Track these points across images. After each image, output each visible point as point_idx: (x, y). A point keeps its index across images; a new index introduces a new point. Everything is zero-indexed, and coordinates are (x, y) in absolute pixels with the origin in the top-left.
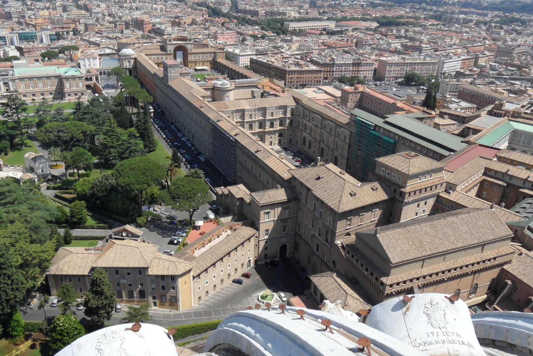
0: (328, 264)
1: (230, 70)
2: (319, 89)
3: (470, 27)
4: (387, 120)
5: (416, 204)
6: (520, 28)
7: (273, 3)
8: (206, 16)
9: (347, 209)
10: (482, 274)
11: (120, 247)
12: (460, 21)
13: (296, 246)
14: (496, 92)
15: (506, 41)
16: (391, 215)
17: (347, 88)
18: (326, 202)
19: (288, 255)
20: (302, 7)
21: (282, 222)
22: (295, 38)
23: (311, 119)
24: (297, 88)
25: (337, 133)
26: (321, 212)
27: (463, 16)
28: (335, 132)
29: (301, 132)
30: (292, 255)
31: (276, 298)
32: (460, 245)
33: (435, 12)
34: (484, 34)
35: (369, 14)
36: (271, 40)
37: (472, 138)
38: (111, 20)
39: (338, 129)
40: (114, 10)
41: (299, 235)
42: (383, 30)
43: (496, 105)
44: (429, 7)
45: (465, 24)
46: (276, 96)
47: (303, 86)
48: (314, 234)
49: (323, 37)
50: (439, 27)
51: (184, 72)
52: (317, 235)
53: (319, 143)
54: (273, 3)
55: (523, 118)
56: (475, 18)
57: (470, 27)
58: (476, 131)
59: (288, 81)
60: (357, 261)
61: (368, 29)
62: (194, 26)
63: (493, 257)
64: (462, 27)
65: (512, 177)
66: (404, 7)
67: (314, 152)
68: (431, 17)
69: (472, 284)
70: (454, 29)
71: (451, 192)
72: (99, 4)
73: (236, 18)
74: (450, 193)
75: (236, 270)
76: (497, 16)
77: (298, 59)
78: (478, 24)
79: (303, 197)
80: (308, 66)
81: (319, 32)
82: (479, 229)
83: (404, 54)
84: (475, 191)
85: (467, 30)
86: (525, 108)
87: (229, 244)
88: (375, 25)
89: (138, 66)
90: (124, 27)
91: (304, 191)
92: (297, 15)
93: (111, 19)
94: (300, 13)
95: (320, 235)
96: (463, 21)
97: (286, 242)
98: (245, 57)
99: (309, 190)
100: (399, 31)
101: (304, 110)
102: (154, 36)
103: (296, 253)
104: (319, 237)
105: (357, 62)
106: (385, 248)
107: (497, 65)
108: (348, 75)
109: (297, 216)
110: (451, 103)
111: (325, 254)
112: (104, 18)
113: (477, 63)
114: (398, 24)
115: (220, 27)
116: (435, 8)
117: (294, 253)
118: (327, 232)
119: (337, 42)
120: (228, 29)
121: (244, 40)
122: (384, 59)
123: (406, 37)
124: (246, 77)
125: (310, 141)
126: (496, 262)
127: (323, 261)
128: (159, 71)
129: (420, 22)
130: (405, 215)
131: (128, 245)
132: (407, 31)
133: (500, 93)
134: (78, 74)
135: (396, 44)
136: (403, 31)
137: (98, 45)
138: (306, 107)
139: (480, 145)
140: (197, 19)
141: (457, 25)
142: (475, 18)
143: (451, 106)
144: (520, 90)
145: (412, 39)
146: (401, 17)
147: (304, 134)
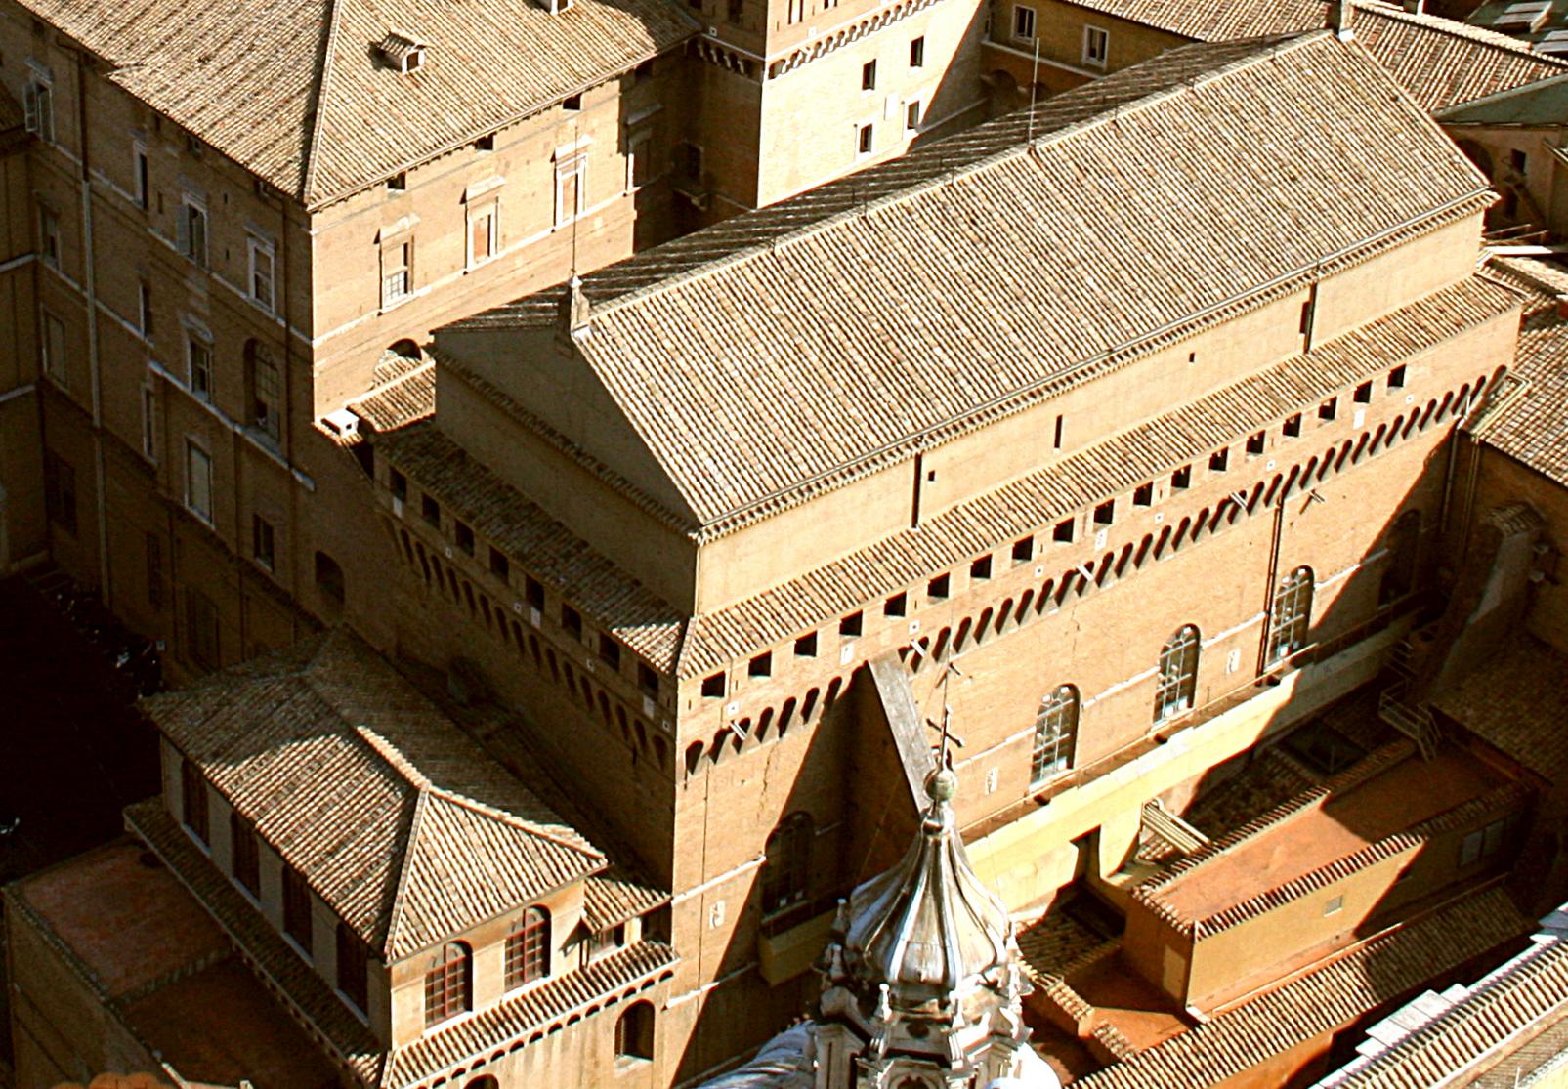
10: (1330, 485)
26: (194, 213)
52: (185, 388)
69: (1272, 575)
79: (61, 125)
91: (56, 78)
95: (201, 380)
99: (90, 64)
104: (201, 399)
109: (35, 267)
118: (250, 351)
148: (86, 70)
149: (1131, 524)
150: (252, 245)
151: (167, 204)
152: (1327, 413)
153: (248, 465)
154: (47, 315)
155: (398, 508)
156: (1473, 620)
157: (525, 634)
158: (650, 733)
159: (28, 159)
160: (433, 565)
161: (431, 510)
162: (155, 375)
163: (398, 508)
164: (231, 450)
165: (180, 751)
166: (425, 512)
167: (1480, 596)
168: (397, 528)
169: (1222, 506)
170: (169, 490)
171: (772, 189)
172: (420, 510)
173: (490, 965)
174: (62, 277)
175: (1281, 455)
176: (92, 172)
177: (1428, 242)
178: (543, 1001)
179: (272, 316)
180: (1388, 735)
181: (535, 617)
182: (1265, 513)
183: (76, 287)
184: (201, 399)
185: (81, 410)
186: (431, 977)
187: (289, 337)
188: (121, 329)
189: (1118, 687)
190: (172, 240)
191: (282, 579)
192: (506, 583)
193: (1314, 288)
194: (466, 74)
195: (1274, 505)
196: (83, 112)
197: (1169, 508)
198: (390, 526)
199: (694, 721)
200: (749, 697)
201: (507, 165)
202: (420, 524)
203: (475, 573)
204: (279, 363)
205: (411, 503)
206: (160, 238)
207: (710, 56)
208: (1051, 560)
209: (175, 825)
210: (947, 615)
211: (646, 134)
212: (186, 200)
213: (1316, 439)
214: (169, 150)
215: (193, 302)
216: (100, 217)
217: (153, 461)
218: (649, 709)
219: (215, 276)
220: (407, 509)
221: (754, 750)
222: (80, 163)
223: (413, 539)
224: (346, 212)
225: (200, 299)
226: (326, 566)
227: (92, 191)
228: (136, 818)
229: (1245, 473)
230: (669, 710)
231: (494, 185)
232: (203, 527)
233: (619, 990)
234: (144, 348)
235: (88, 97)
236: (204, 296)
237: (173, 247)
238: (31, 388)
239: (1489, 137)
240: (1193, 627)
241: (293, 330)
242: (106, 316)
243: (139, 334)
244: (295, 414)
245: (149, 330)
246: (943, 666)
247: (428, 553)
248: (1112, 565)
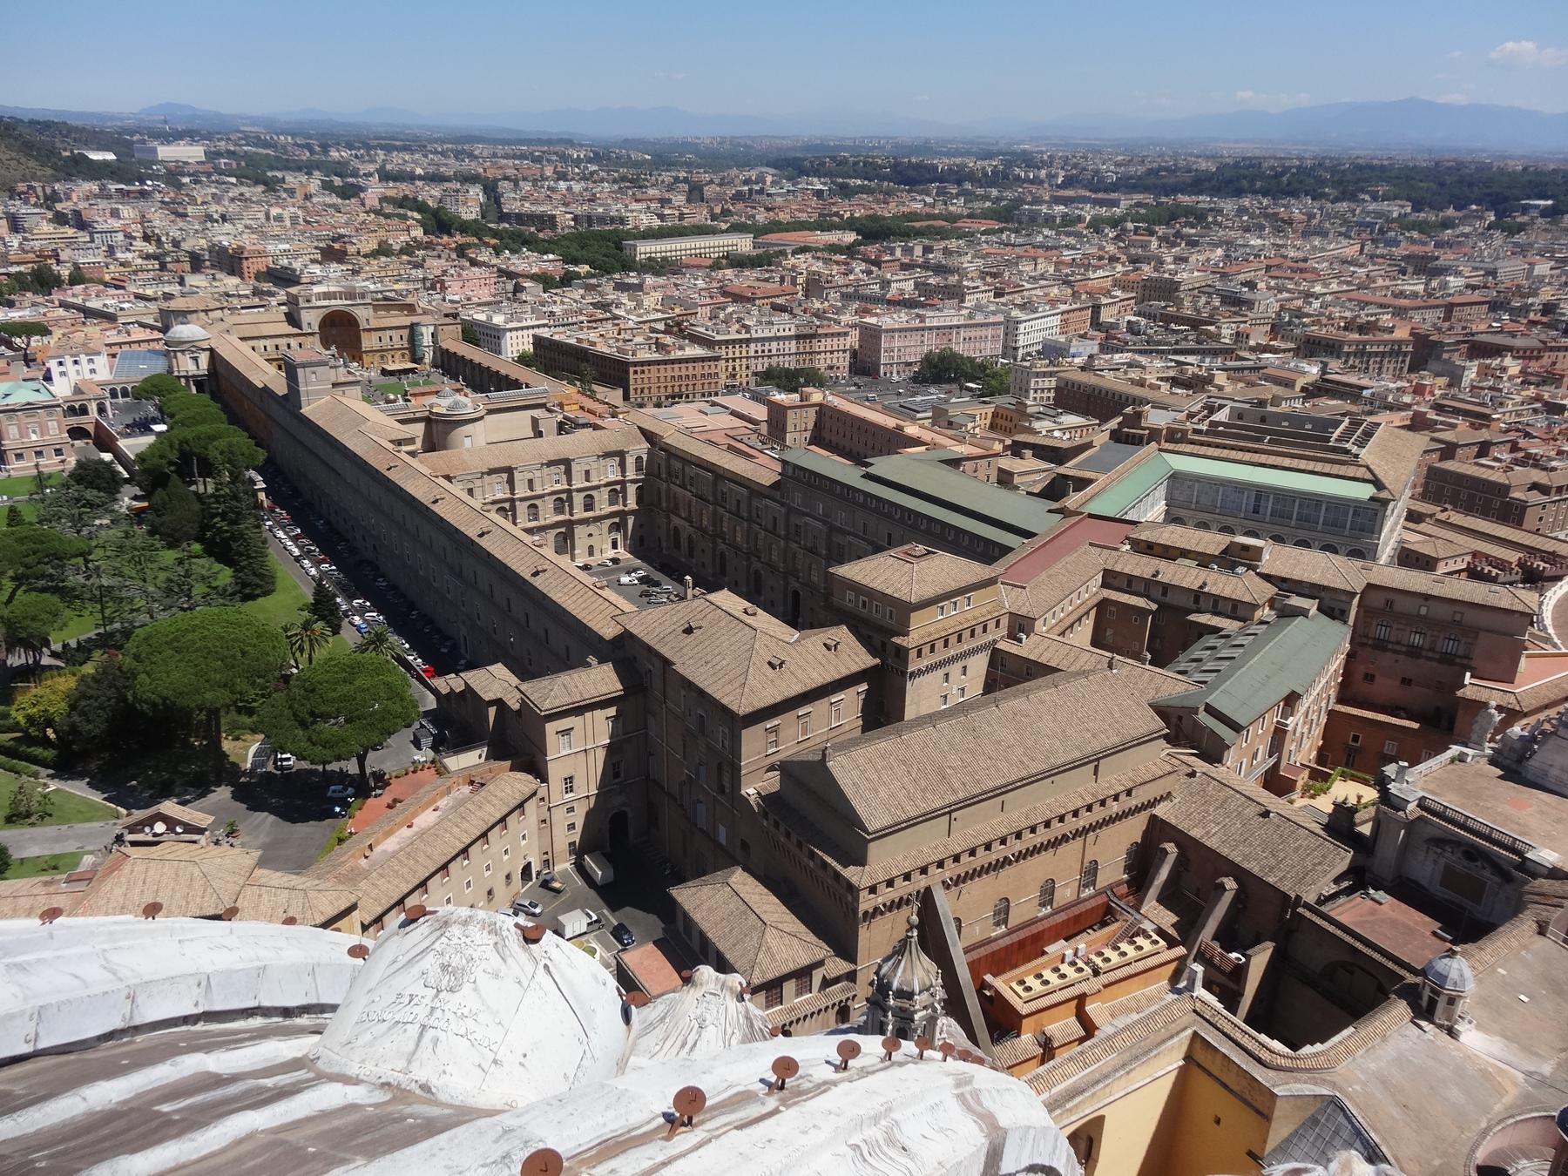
1: (485, 374)
2: (714, 404)
3: (1078, 235)
4: (870, 470)
5: (940, 673)
6: (1193, 231)
7: (594, 195)
8: (418, 233)
10: (1104, 832)
11: (140, 867)
12: (1054, 221)
14: (1143, 386)
15: (1162, 263)
17: (780, 397)
18: (709, 691)
20: (669, 201)
22: (650, 280)
23: (687, 480)
24: (658, 405)
25: (754, 512)
27: (1062, 207)
28: (750, 512)
29: (668, 517)
31: (601, 956)
32: (1035, 767)
33: (999, 199)
34: (1111, 249)
35: (836, 214)
36: (590, 288)
37: (1073, 500)
38: (151, 251)
39: (755, 503)
40: (159, 220)
42: (872, 250)
43: (1125, 415)
44: (980, 191)
45: (1066, 226)
46: (596, 427)
47: (675, 398)
49: (720, 274)
50: (1004, 236)
51: (343, 379)
53: (714, 542)
54: (594, 195)
55: (1193, 442)
56: (1088, 212)
57: (1078, 235)
58: (1081, 484)
59: (636, 389)
60: (788, 835)
61: (834, 248)
62: (383, 259)
63: (1122, 788)
64: (1058, 234)
65: (1166, 588)
66: (920, 193)
67: (703, 565)
68: (985, 215)
70: (1040, 239)
71: (1024, 637)
72: (117, 209)
73: (495, 234)
74: (1020, 641)
75: (490, 893)
76: (1139, 205)
77: (658, 332)
78: (1096, 225)
80: (681, 348)
81: (709, 262)
83: (923, 306)
84: (1086, 630)
85: (1071, 240)
86: (1195, 420)
87: (465, 825)
88: (850, 237)
89: (221, 370)
90: (187, 267)
92: (657, 223)
93: (151, 249)
94: (661, 217)
96: (1063, 220)
98: (520, 333)
100: (908, 251)
101: (668, 460)
102: (273, 289)
105: (806, 331)
106: (849, 792)
107: (1143, 321)
108: (790, 363)
109: (647, 734)
110: (1038, 419)
112: (131, 245)
113: (1098, 318)
114: (907, 234)
115: (454, 260)
116: (994, 192)
118: (720, 767)
119: (757, 284)
120: (474, 263)
121: (518, 289)
122: (872, 320)
123: (925, 266)
124: (516, 385)
125: (690, 540)
126: (1133, 802)
128: (275, 380)
129: (961, 228)
131: (169, 857)
132: (927, 250)
133: (1152, 386)
134: (42, 398)
135: (904, 285)
136: (918, 251)
137: (110, 318)
138: (673, 451)
139: (1091, 516)
140: (390, 242)
141: (1046, 232)
142: (1088, 212)
143: (1037, 425)
144: (1198, 376)
145: (940, 269)
146: (913, 216)
147: (676, 521)
149: (1029, 840)
161: (776, 825)
171: (910, 712)
181: (812, 864)
182: (1079, 840)
199: (866, 903)
200: (886, 895)
202: (772, 829)
208: (999, 852)
218: (850, 898)
229: (1072, 824)
230: (856, 899)
245: (685, 758)
248: (1022, 856)
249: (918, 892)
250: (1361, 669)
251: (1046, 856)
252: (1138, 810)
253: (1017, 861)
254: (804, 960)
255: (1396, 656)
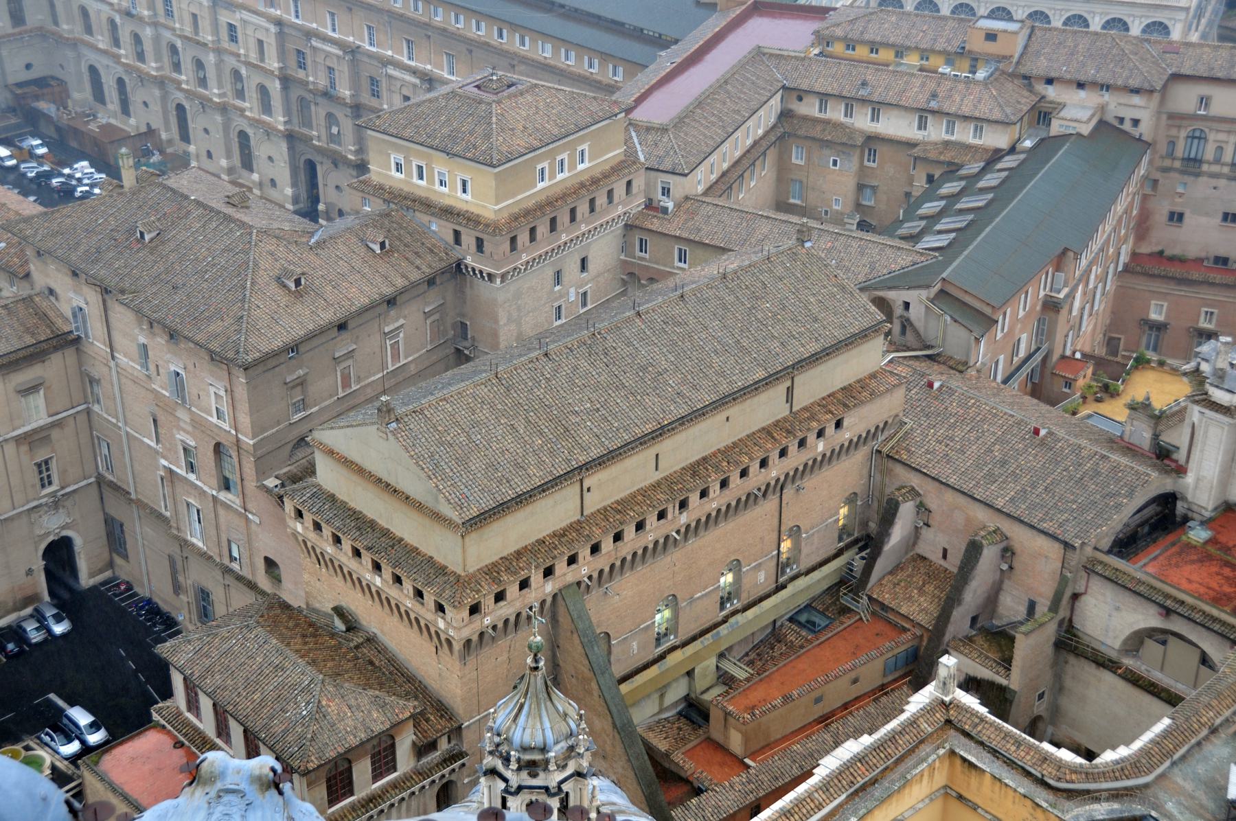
0: (250, 577)
9: (277, 343)
10: (809, 483)
13: (115, 537)
16: (465, 338)
19: (86, 579)
21: (24, 448)
30: (108, 574)
41: (115, 488)
48: (171, 471)
52: (181, 471)
82: (766, 326)
95: (191, 467)
97: (63, 528)
103: (119, 561)
104: (192, 477)
109: (88, 412)
111: (229, 542)
117: (111, 565)
118: (218, 448)
126: (846, 435)
127: (227, 571)
130: (513, 327)
148: (106, 296)
150: (212, 390)
151: (161, 370)
152: (802, 443)
153: (221, 512)
154: (99, 438)
155: (299, 528)
156: (887, 548)
157: (373, 590)
158: (443, 637)
159: (77, 349)
160: (320, 558)
161: (317, 527)
162: (164, 466)
163: (299, 528)
164: (212, 504)
165: (182, 673)
166: (315, 529)
167: (889, 535)
168: (300, 539)
169: (749, 495)
170: (178, 529)
172: (311, 528)
173: (362, 770)
174: (105, 416)
175: (776, 470)
176: (116, 355)
177: (855, 352)
178: (395, 785)
179: (228, 429)
180: (845, 611)
183: (114, 421)
184: (192, 477)
185: (124, 490)
186: (328, 780)
187: (238, 440)
188: (143, 442)
189: (699, 594)
190: (166, 390)
191: (246, 573)
192: (361, 563)
193: (793, 378)
194: (329, 288)
195: (779, 494)
196: (107, 321)
197: (717, 499)
198: (296, 539)
201: (357, 337)
202: (312, 536)
203: (344, 559)
204: (234, 454)
205: (306, 525)
206: (160, 390)
207: (468, 272)
209: (179, 714)
210: (602, 562)
211: (436, 317)
212: (173, 368)
213: (796, 459)
214: (159, 339)
215: (182, 424)
216: (124, 380)
217: (168, 514)
219: (193, 409)
220: (305, 528)
221: (503, 643)
222: (109, 350)
223: (309, 545)
224: (265, 369)
225: (185, 422)
226: (270, 564)
227: (117, 365)
228: (159, 712)
231: (350, 349)
232: (199, 549)
233: (436, 776)
234: (157, 452)
235: (109, 312)
236: (188, 420)
237: (167, 394)
238: (92, 480)
239: (891, 295)
240: (738, 560)
241: (240, 436)
242: (133, 436)
243: (153, 444)
244: (245, 483)
245: (158, 441)
246: (602, 590)
247: (318, 551)
249: (543, 603)
250: (1162, 209)
251: (725, 528)
252: (853, 445)
253: (686, 538)
254: (379, 722)
255: (1214, 182)
